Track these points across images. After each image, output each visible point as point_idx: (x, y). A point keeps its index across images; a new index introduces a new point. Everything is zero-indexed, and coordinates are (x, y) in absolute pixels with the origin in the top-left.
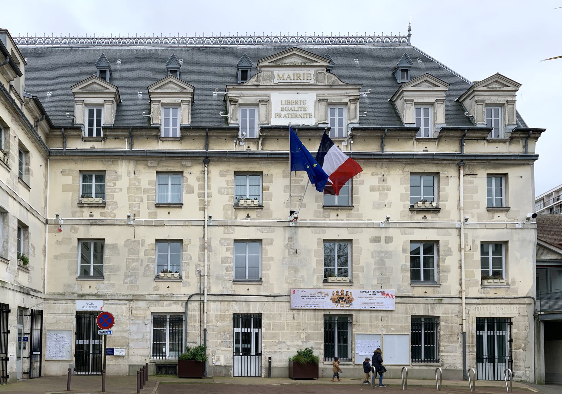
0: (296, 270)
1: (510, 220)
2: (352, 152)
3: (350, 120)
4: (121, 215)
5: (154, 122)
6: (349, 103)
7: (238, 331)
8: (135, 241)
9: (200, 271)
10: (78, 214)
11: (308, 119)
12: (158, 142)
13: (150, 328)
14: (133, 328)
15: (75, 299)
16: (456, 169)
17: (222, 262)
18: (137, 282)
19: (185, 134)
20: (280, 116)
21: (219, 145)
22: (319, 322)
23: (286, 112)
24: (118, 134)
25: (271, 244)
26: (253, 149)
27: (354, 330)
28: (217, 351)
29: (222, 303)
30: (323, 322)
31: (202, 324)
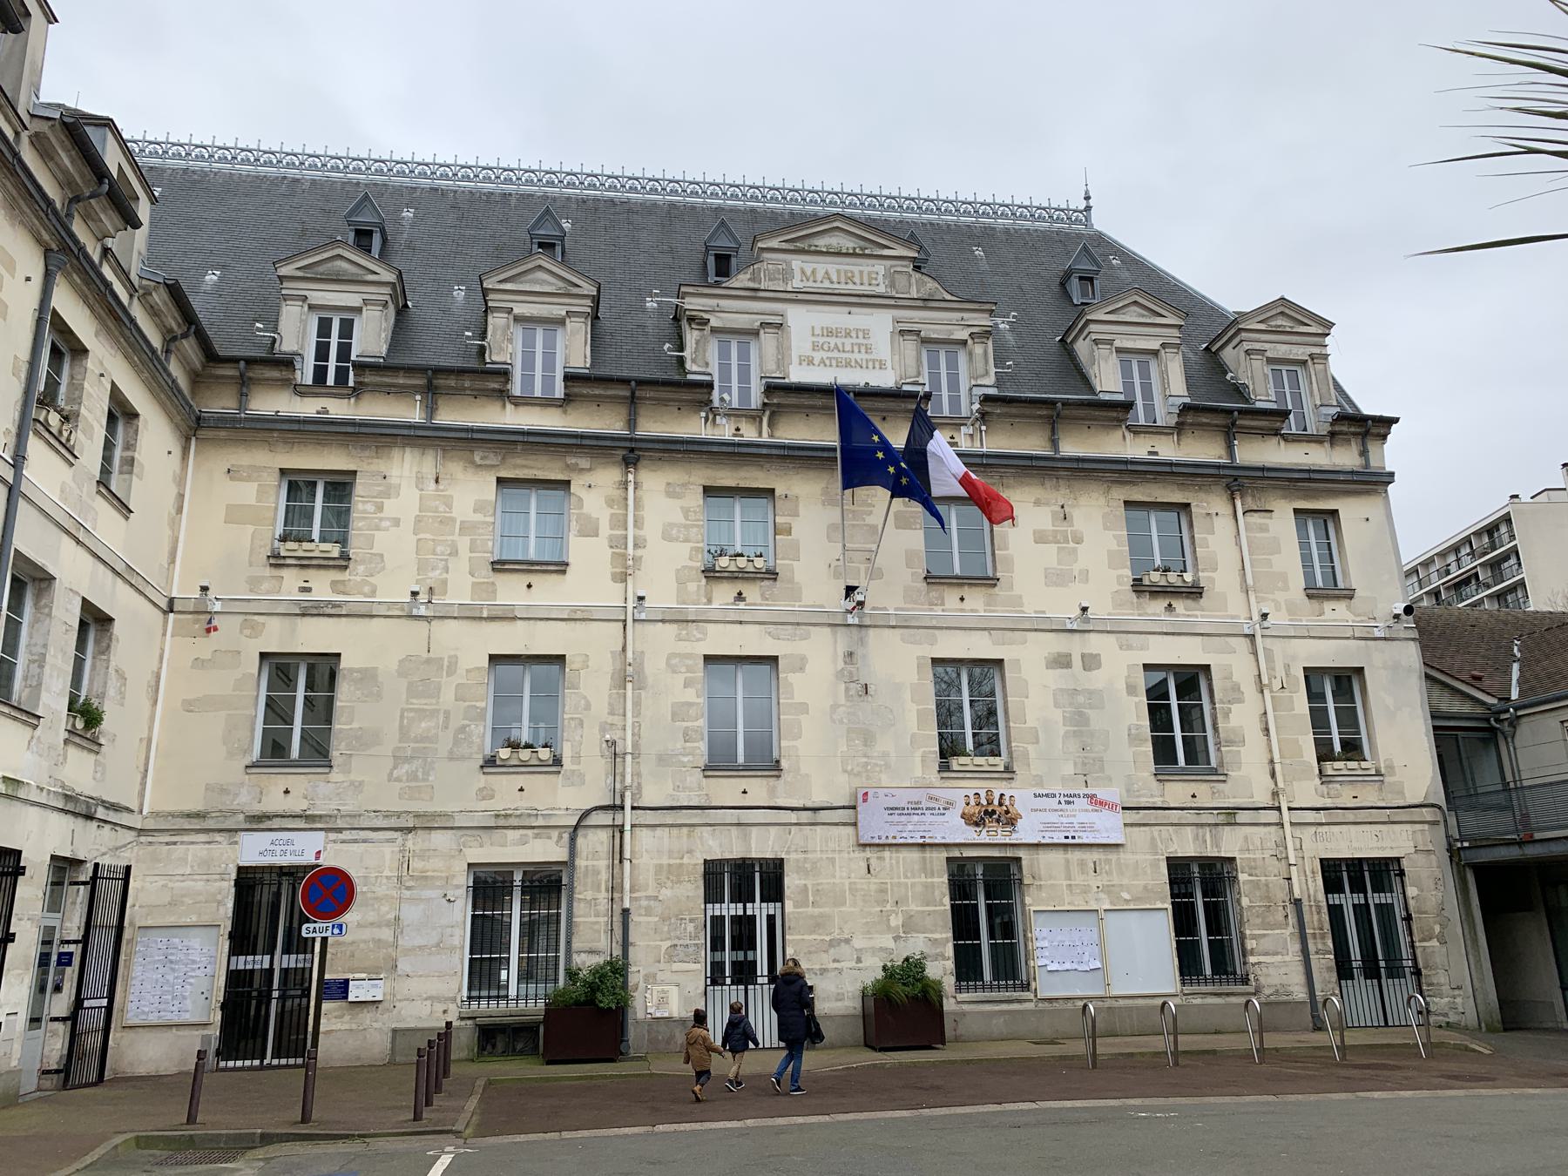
0: (868, 738)
1: (1358, 619)
2: (985, 450)
3: (976, 379)
4: (393, 589)
5: (495, 358)
6: (970, 342)
7: (717, 913)
8: (428, 661)
9: (614, 743)
10: (265, 586)
11: (877, 372)
12: (504, 406)
13: (461, 913)
14: (411, 914)
15: (236, 831)
16: (1225, 498)
17: (674, 715)
18: (428, 775)
19: (576, 390)
20: (811, 362)
21: (663, 422)
22: (936, 880)
23: (825, 355)
24: (395, 381)
25: (802, 669)
26: (749, 434)
27: (1028, 900)
28: (660, 976)
29: (675, 831)
30: (945, 879)
31: (616, 895)
